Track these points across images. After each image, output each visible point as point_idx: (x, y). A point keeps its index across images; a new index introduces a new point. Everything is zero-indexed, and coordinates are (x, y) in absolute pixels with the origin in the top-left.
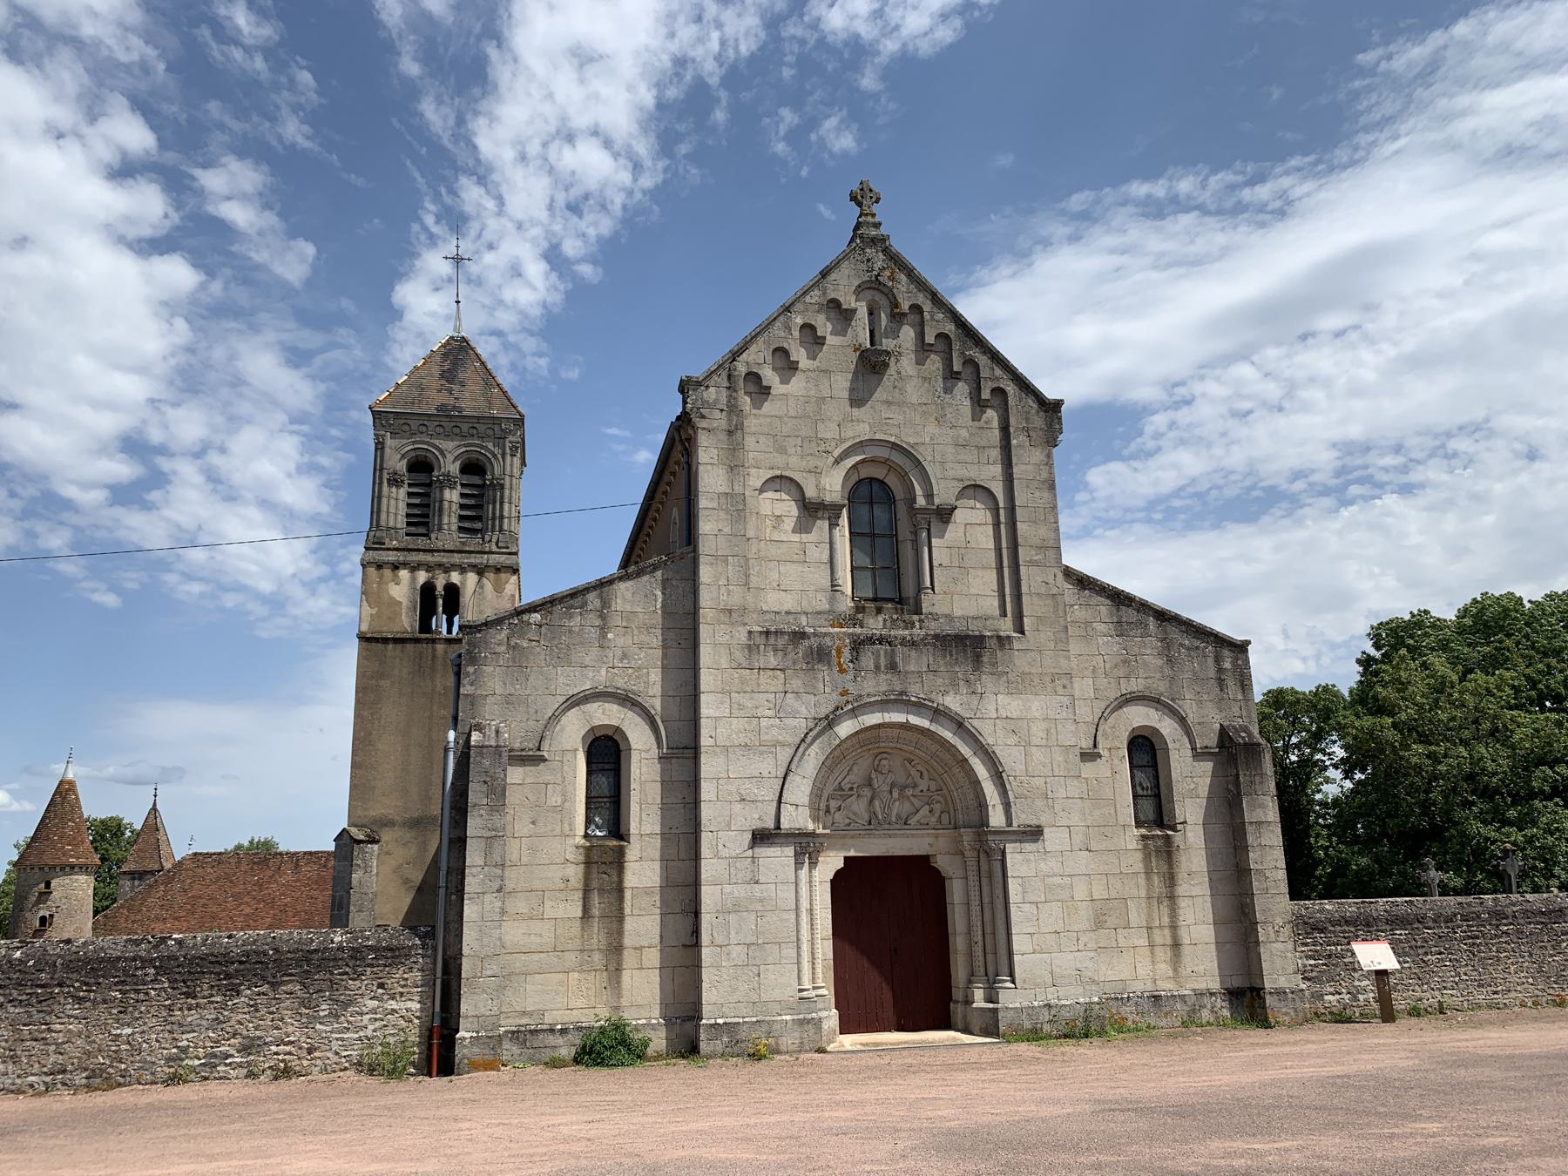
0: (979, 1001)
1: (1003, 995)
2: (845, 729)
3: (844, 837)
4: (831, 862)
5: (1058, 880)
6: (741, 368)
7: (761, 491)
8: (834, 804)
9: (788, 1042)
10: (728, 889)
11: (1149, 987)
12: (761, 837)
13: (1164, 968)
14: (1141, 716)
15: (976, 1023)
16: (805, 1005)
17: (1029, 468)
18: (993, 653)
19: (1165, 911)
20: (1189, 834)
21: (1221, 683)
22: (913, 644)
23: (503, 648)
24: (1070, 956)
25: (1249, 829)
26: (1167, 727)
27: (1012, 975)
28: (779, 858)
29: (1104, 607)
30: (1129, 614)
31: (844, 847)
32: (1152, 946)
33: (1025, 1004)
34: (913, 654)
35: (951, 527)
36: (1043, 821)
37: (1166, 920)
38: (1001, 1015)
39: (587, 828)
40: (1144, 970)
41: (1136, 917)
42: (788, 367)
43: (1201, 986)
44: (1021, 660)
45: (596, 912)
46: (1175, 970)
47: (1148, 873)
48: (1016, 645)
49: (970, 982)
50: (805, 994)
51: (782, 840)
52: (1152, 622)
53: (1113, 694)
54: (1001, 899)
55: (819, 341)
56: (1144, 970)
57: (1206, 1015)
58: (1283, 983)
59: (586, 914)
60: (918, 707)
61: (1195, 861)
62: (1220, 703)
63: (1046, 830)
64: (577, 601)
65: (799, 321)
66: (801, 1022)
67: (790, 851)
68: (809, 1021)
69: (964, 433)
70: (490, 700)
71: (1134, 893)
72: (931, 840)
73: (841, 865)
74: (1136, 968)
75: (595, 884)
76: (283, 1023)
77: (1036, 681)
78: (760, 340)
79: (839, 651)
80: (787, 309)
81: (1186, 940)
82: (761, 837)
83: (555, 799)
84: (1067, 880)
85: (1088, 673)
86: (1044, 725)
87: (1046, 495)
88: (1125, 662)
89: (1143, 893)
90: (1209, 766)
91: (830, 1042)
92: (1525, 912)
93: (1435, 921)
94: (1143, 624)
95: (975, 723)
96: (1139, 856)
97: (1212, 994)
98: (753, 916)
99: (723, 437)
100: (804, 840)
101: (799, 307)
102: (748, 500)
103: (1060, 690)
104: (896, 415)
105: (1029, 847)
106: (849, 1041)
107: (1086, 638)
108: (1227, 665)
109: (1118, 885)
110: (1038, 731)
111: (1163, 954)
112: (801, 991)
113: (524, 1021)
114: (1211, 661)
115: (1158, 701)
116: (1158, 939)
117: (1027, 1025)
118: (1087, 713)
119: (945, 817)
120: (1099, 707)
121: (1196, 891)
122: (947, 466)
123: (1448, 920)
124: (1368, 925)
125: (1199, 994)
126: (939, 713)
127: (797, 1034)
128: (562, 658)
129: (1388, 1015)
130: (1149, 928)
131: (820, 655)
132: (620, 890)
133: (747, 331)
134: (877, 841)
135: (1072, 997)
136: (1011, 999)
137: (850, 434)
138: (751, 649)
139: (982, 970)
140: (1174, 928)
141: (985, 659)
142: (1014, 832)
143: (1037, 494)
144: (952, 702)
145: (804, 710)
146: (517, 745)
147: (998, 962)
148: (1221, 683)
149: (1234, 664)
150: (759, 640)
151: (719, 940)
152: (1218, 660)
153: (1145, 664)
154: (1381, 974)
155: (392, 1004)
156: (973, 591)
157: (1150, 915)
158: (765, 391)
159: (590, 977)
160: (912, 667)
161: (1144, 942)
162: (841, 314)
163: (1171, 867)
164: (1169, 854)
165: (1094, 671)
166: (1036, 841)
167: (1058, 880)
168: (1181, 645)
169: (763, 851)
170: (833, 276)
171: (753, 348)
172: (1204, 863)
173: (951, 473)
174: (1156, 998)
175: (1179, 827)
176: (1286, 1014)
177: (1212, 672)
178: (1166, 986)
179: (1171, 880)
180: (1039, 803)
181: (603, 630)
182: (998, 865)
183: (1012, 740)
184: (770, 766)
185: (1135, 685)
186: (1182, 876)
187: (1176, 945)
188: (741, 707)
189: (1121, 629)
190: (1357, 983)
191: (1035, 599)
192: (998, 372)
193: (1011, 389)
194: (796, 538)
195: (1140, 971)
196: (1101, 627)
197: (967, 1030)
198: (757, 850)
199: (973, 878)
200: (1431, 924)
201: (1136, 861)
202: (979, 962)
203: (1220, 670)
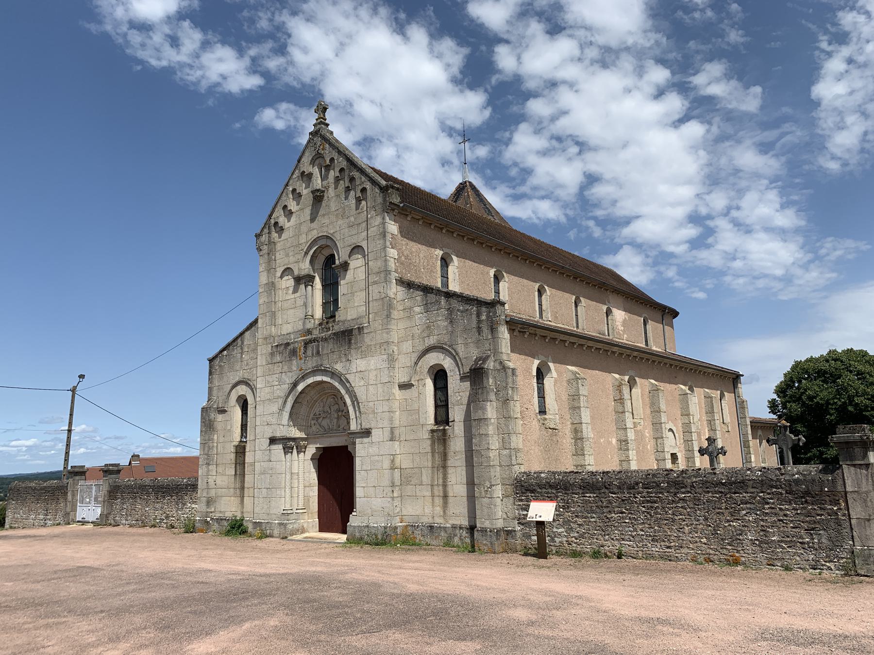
2: (300, 387)
4: (311, 450)
5: (376, 458)
6: (273, 221)
7: (281, 277)
8: (313, 422)
9: (276, 532)
10: (262, 464)
12: (273, 441)
13: (438, 510)
14: (434, 358)
18: (356, 338)
19: (441, 476)
20: (456, 428)
21: (479, 330)
22: (326, 339)
24: (379, 500)
25: (474, 424)
26: (447, 363)
29: (418, 295)
30: (432, 297)
31: (315, 443)
32: (433, 496)
35: (348, 272)
36: (372, 426)
37: (441, 481)
40: (428, 510)
41: (426, 478)
42: (289, 214)
43: (457, 522)
44: (367, 339)
46: (444, 512)
47: (433, 452)
48: (365, 331)
52: (443, 301)
53: (421, 348)
55: (300, 195)
56: (428, 510)
57: (456, 540)
58: (487, 524)
59: (236, 474)
60: (325, 372)
61: (458, 444)
63: (373, 431)
64: (235, 344)
67: (281, 446)
69: (352, 219)
72: (346, 438)
74: (421, 508)
76: (154, 510)
81: (451, 494)
82: (273, 441)
83: (229, 428)
85: (410, 338)
86: (374, 373)
87: (382, 241)
88: (428, 327)
89: (430, 465)
90: (467, 384)
91: (292, 535)
92: (704, 483)
96: (429, 442)
97: (461, 528)
99: (266, 256)
101: (291, 182)
102: (277, 284)
103: (383, 352)
104: (326, 221)
105: (366, 440)
108: (484, 317)
109: (418, 460)
110: (372, 376)
111: (439, 501)
114: (474, 317)
115: (443, 348)
116: (436, 493)
118: (405, 360)
120: (414, 357)
121: (458, 463)
123: (631, 487)
124: (566, 489)
125: (454, 527)
126: (333, 374)
129: (541, 552)
130: (432, 486)
131: (294, 353)
132: (244, 463)
133: (273, 205)
135: (378, 522)
138: (272, 354)
140: (445, 486)
141: (353, 341)
143: (378, 242)
144: (339, 367)
145: (289, 379)
148: (479, 330)
149: (488, 316)
150: (275, 350)
152: (478, 315)
153: (439, 326)
154: (540, 524)
155: (193, 506)
156: (356, 304)
157: (433, 478)
158: (282, 229)
160: (325, 352)
161: (429, 494)
162: (307, 177)
163: (445, 449)
164: (445, 440)
168: (458, 310)
169: (274, 447)
172: (463, 446)
173: (347, 243)
174: (431, 527)
175: (450, 424)
178: (439, 521)
179: (445, 456)
180: (371, 416)
181: (242, 353)
183: (362, 383)
184: (275, 408)
185: (432, 341)
186: (450, 454)
187: (445, 496)
190: (555, 530)
192: (363, 178)
193: (368, 186)
194: (293, 296)
195: (426, 511)
200: (615, 490)
201: (427, 446)
203: (479, 322)
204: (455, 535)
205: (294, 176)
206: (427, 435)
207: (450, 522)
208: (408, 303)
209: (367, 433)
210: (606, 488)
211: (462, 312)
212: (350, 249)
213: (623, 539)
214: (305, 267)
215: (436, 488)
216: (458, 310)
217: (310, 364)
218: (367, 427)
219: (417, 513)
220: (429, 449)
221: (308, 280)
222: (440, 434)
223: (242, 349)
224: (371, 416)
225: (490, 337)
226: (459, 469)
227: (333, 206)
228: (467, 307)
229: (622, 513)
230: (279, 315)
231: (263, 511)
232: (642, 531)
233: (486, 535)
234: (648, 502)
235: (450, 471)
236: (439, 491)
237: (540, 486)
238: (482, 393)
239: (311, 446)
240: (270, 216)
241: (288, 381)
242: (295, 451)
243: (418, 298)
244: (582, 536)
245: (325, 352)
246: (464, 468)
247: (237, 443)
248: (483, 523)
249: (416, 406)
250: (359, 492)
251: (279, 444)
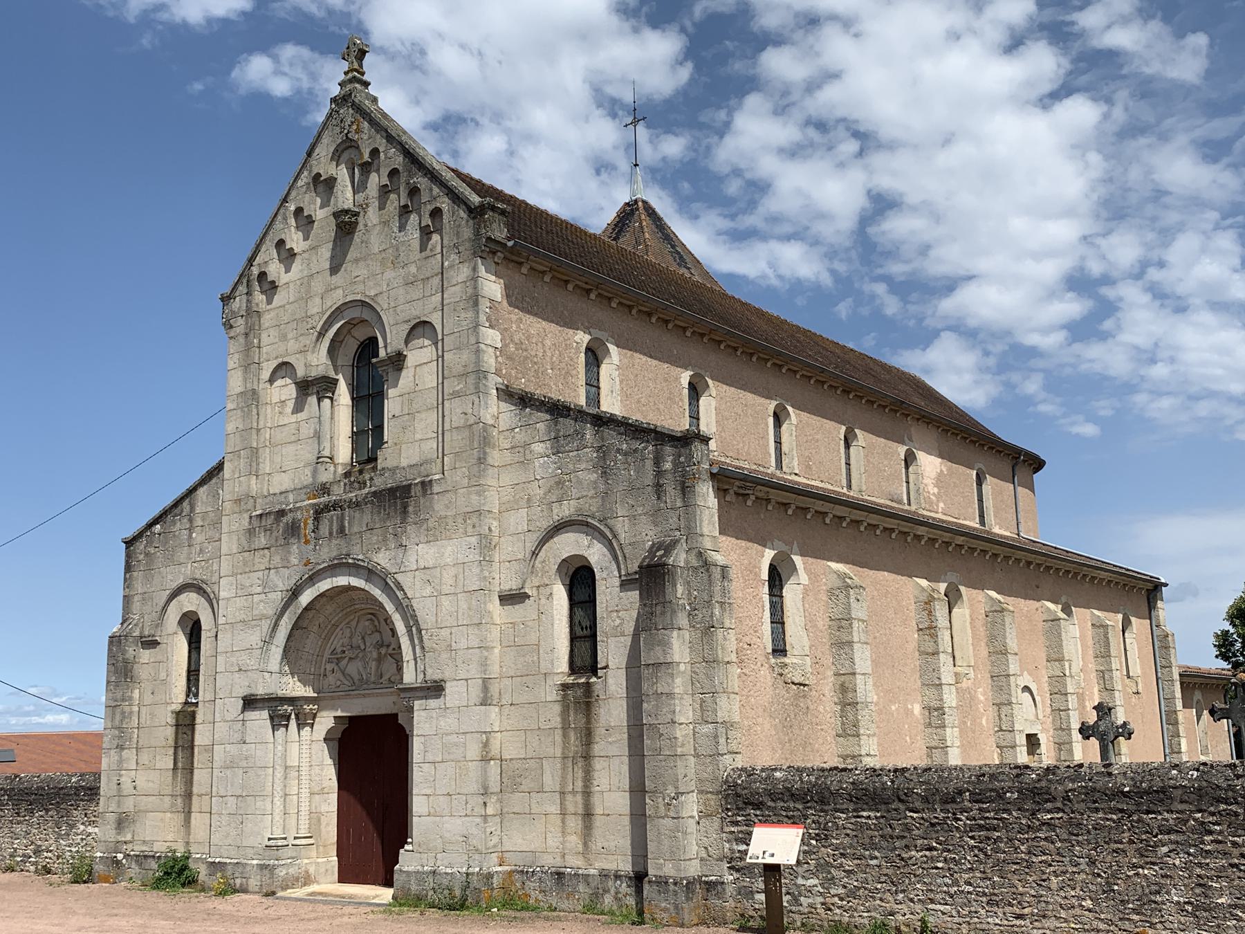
2: (305, 598)
3: (333, 698)
4: (326, 721)
5: (453, 738)
6: (255, 271)
7: (271, 381)
8: (329, 667)
9: (253, 883)
11: (558, 862)
12: (250, 703)
13: (574, 841)
14: (570, 544)
17: (458, 288)
19: (580, 774)
20: (610, 681)
21: (659, 489)
22: (358, 504)
23: (141, 557)
24: (459, 821)
25: (645, 672)
26: (596, 554)
28: (260, 718)
29: (541, 421)
30: (567, 425)
31: (334, 708)
32: (563, 814)
34: (357, 515)
35: (404, 373)
36: (447, 674)
37: (579, 785)
39: (188, 696)
40: (553, 842)
41: (551, 780)
42: (288, 256)
43: (611, 865)
44: (439, 505)
45: (180, 765)
46: (585, 844)
47: (565, 728)
48: (436, 489)
50: (272, 843)
52: (589, 432)
53: (545, 524)
55: (310, 221)
56: (553, 842)
57: (608, 900)
58: (669, 870)
59: (175, 768)
60: (355, 568)
61: (615, 713)
62: (656, 515)
63: (449, 687)
64: (177, 511)
65: (293, 208)
67: (265, 714)
69: (413, 269)
70: (136, 598)
71: (550, 751)
72: (394, 698)
75: (180, 743)
77: (450, 522)
78: (268, 238)
79: (306, 524)
80: (285, 200)
81: (598, 810)
82: (250, 703)
83: (163, 675)
84: (461, 738)
85: (523, 503)
86: (453, 571)
87: (470, 314)
88: (558, 483)
89: (559, 753)
90: (635, 595)
92: (1089, 792)
93: (925, 800)
94: (580, 434)
95: (399, 577)
96: (557, 708)
97: (617, 877)
98: (241, 771)
99: (242, 340)
100: (275, 704)
101: (293, 194)
102: (261, 393)
103: (470, 529)
104: (361, 271)
105: (433, 703)
107: (524, 463)
108: (668, 466)
110: (448, 578)
111: (575, 823)
112: (269, 839)
113: (144, 848)
114: (649, 464)
115: (587, 524)
116: (571, 808)
118: (512, 548)
120: (532, 541)
121: (613, 750)
122: (398, 309)
123: (949, 800)
124: (822, 801)
125: (604, 875)
126: (371, 573)
128: (171, 560)
130: (562, 793)
131: (293, 530)
132: (192, 747)
133: (257, 238)
134: (356, 701)
135: (453, 865)
137: (329, 304)
138: (251, 532)
140: (587, 794)
141: (411, 509)
143: (463, 315)
144: (383, 559)
145: (283, 582)
146: (146, 633)
148: (659, 489)
149: (676, 464)
150: (256, 523)
151: (222, 793)
152: (658, 461)
153: (579, 482)
154: (772, 870)
155: (90, 829)
156: (418, 436)
157: (564, 778)
159: (175, 816)
160: (355, 529)
161: (554, 809)
162: (325, 186)
163: (588, 722)
164: (588, 705)
165: (529, 500)
166: (438, 697)
167: (453, 738)
168: (618, 451)
170: (317, 151)
171: (263, 249)
172: (624, 716)
174: (560, 875)
175: (600, 673)
176: (665, 910)
177: (649, 478)
178: (574, 862)
179: (588, 736)
180: (444, 656)
181: (191, 530)
183: (428, 591)
184: (254, 638)
185: (566, 510)
186: (599, 732)
187: (588, 815)
188: (243, 587)
189: (558, 445)
190: (800, 881)
191: (455, 432)
192: (436, 190)
193: (445, 204)
194: (294, 418)
195: (550, 842)
196: (539, 448)
198: (246, 714)
200: (918, 805)
201: (553, 715)
203: (659, 473)
204: (606, 891)
205: (300, 183)
206: (553, 695)
207: (597, 865)
208: (520, 436)
209: (435, 689)
210: (901, 800)
211: (626, 454)
212: (407, 327)
213: (932, 901)
214: (318, 362)
215: (569, 797)
216: (618, 451)
217: (326, 552)
218: (437, 677)
219: (532, 848)
220: (557, 721)
221: (324, 387)
222: (580, 692)
223: (191, 521)
224: (444, 656)
225: (679, 504)
226: (616, 761)
227: (376, 242)
228: (636, 445)
229: (931, 849)
230: (265, 454)
231: (229, 841)
232: (970, 884)
233: (667, 891)
234: (981, 827)
235: (598, 764)
236: (575, 803)
237: (773, 796)
238: (663, 613)
239: (324, 713)
240: (251, 261)
241: (281, 586)
242: (293, 723)
243: (541, 426)
244: (852, 894)
245: (355, 529)
246: (626, 760)
247: (178, 707)
248: (660, 867)
249: (533, 638)
250: (419, 805)
251: (262, 709)
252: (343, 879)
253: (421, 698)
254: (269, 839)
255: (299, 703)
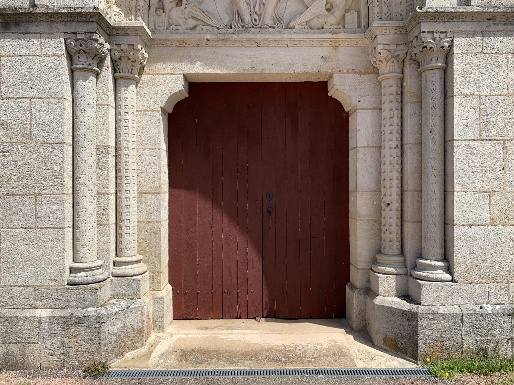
0: (387, 295)
1: (428, 293)
4: (164, 83)
15: (378, 329)
16: (77, 294)
27: (447, 258)
33: (470, 308)
38: (422, 324)
49: (375, 262)
50: (80, 277)
51: (42, 27)
54: (437, 131)
66: (65, 322)
67: (56, 46)
68: (79, 321)
72: (325, 51)
73: (178, 85)
91: (119, 353)
100: (82, 28)
106: (173, 339)
117: (470, 343)
119: (352, 18)
127: (57, 341)
134: (237, 52)
136: (441, 299)
139: (396, 245)
142: (475, 17)
147: (427, 238)
182: (434, 80)
197: (364, 335)
199: (390, 107)
202: (391, 234)
239: (163, 67)
242: (107, 73)
251: (51, 35)
252: (183, 311)
253: (474, 34)
254: (72, 270)
255: (125, 41)
